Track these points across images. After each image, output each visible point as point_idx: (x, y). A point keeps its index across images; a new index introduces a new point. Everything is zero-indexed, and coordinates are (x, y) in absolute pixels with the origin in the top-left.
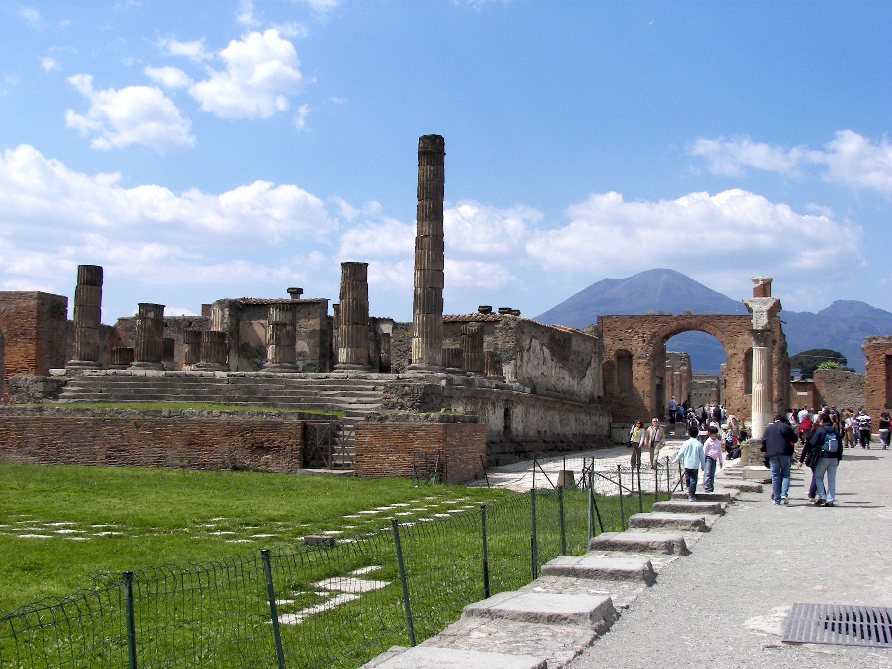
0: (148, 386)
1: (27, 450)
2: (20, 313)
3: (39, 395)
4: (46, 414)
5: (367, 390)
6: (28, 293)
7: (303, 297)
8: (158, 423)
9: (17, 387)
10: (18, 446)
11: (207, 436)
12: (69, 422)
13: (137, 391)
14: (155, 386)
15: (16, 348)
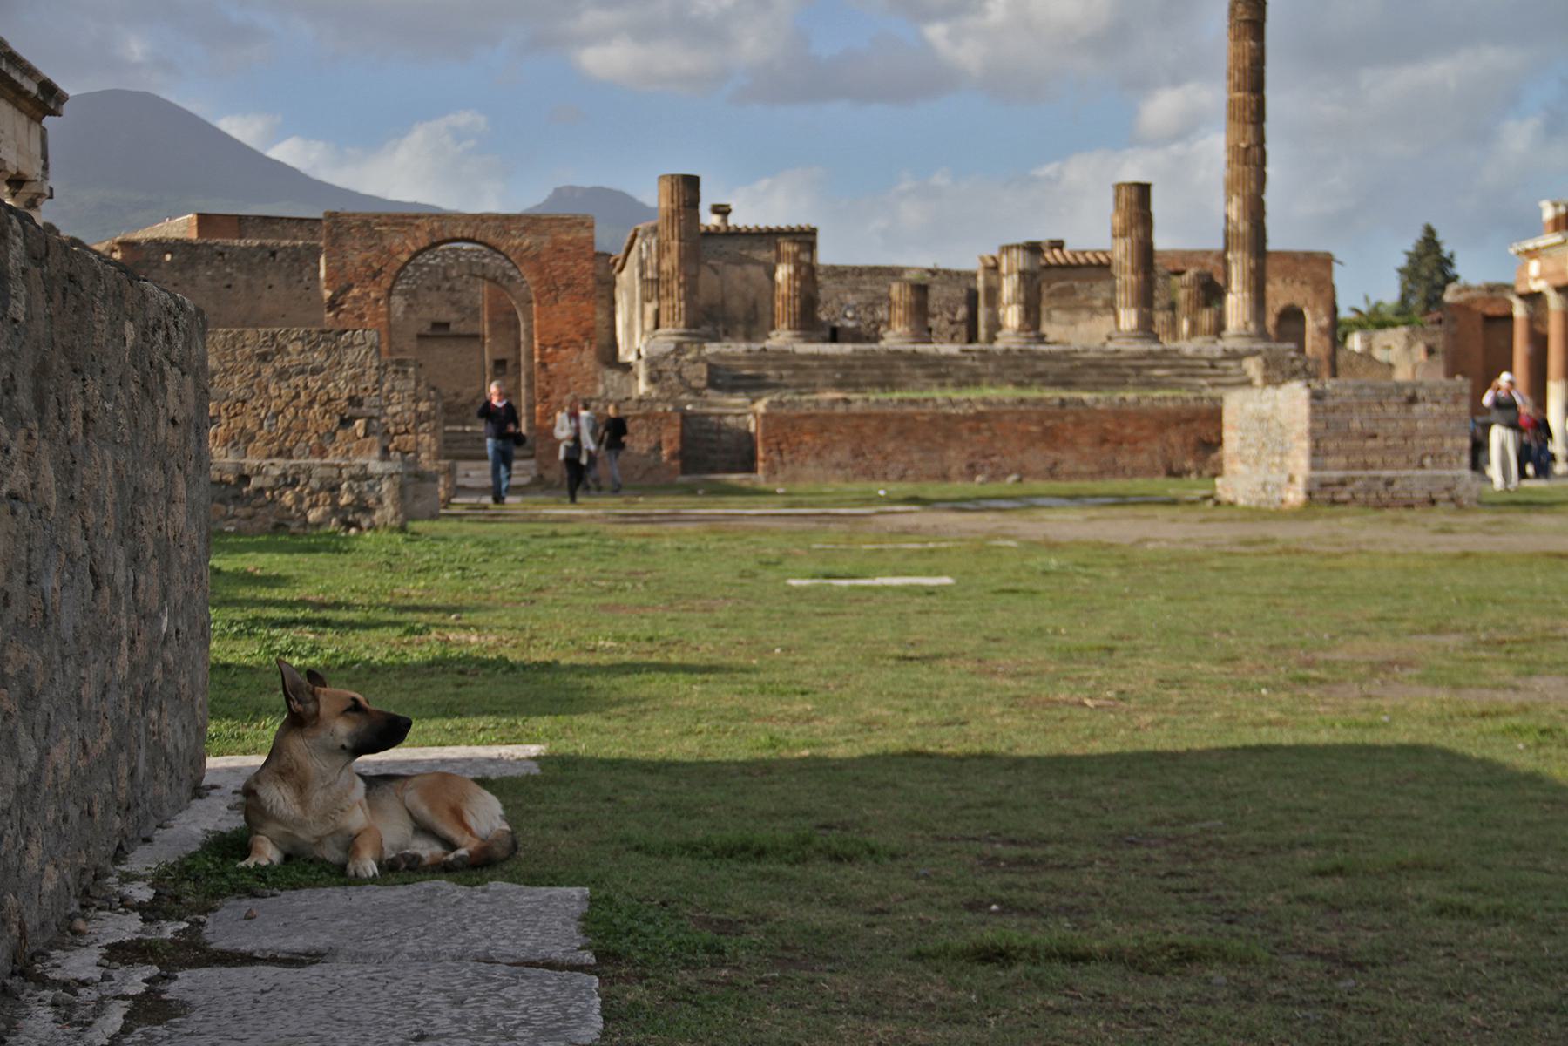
0: (852, 367)
1: (834, 460)
2: (561, 251)
3: (703, 383)
4: (856, 408)
5: (1202, 367)
6: (575, 217)
7: (733, 220)
8: (1050, 416)
9: (660, 372)
10: (818, 455)
11: (1128, 431)
12: (903, 418)
13: (846, 376)
14: (863, 367)
15: (555, 308)
